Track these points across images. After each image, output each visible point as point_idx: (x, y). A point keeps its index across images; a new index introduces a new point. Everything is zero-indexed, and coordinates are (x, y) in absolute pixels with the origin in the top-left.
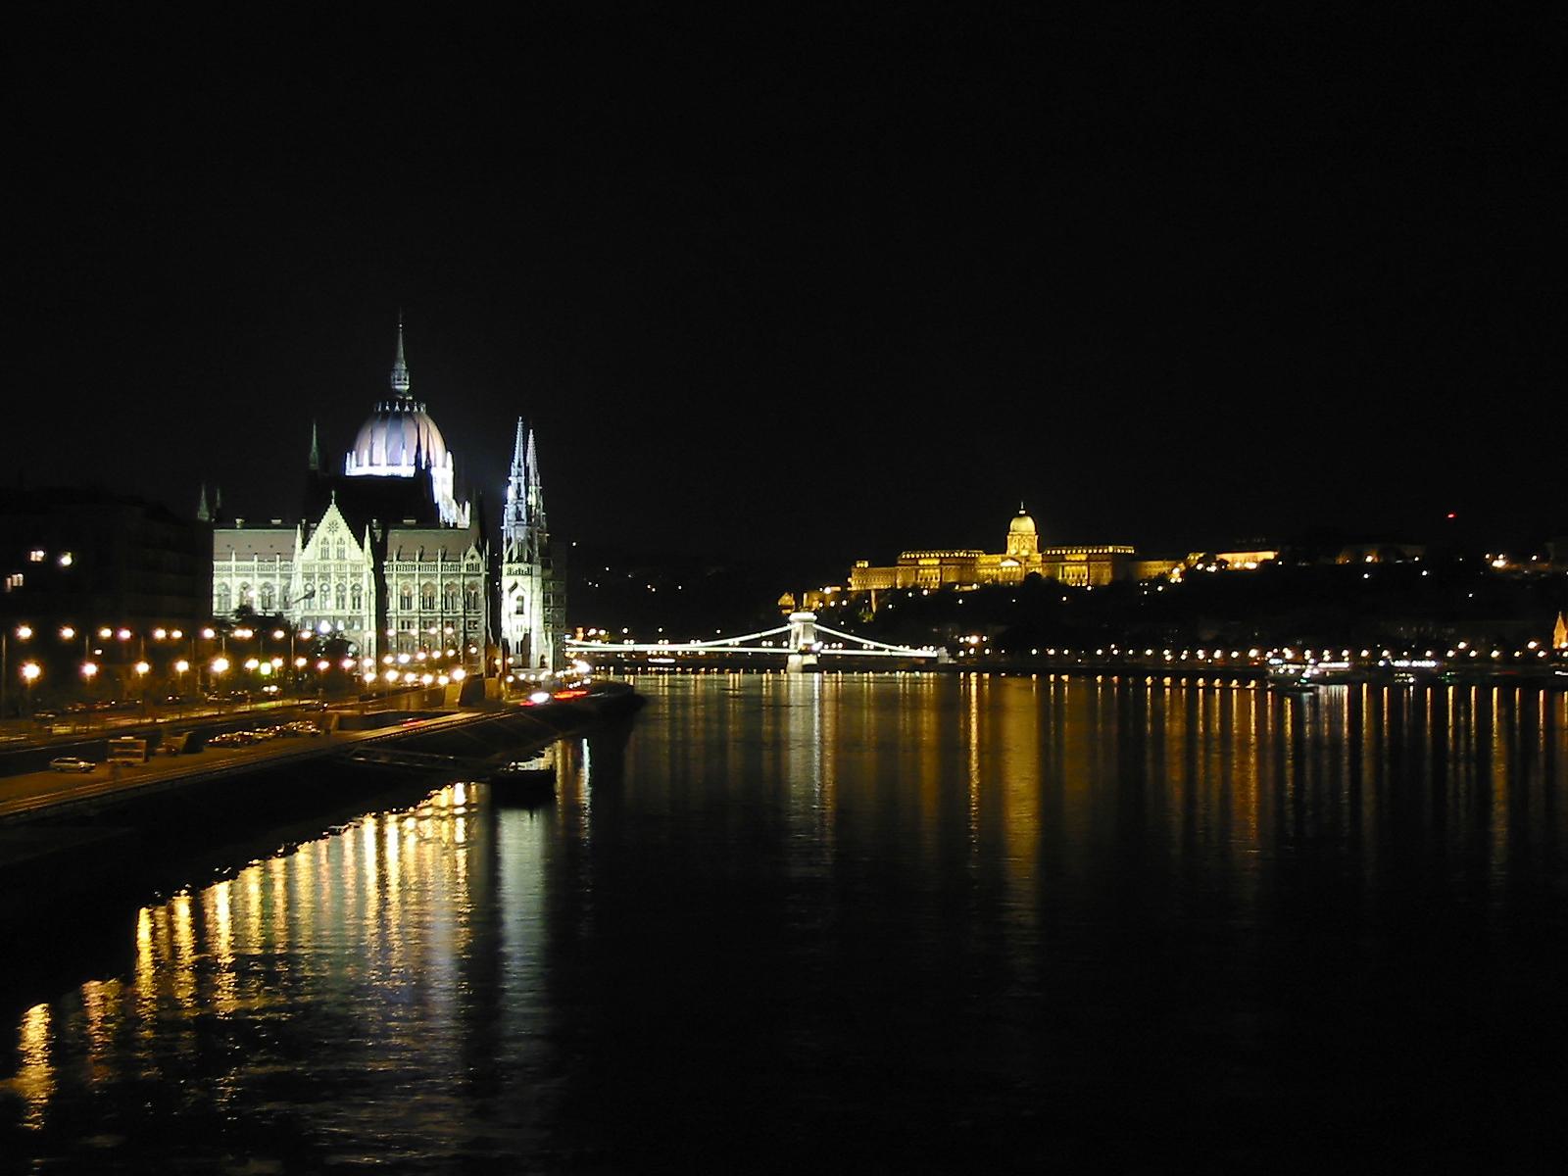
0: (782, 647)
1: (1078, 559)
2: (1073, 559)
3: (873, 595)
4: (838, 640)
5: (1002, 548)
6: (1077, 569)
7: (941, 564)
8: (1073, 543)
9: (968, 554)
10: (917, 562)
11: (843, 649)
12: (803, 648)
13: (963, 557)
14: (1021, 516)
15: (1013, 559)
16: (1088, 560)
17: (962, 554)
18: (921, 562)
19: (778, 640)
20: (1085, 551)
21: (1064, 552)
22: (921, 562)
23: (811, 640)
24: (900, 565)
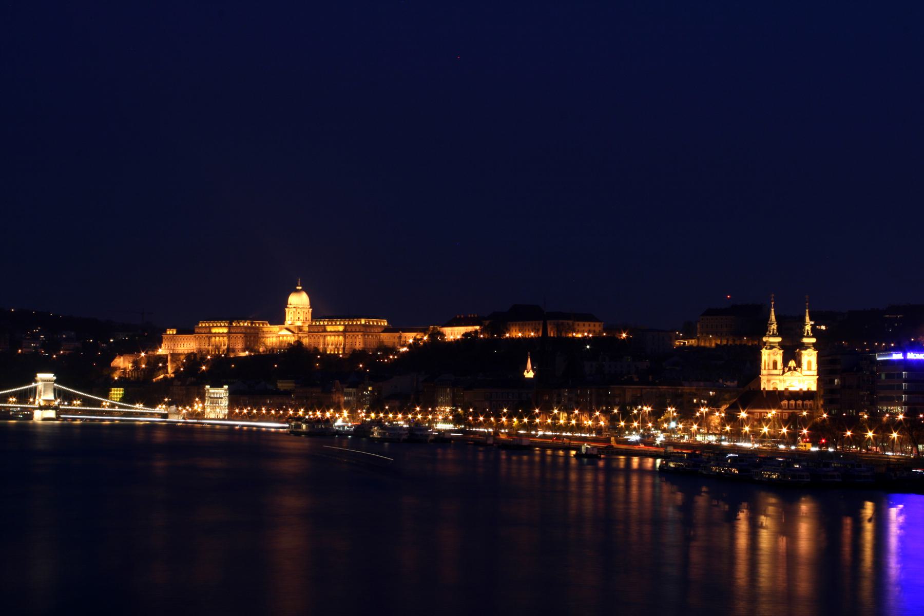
0: (31, 403)
3: (169, 358)
4: (76, 397)
6: (334, 339)
7: (229, 332)
8: (332, 317)
9: (252, 324)
11: (83, 405)
12: (42, 404)
14: (297, 291)
15: (287, 329)
16: (345, 331)
18: (214, 330)
19: (23, 397)
22: (214, 330)
23: (51, 396)
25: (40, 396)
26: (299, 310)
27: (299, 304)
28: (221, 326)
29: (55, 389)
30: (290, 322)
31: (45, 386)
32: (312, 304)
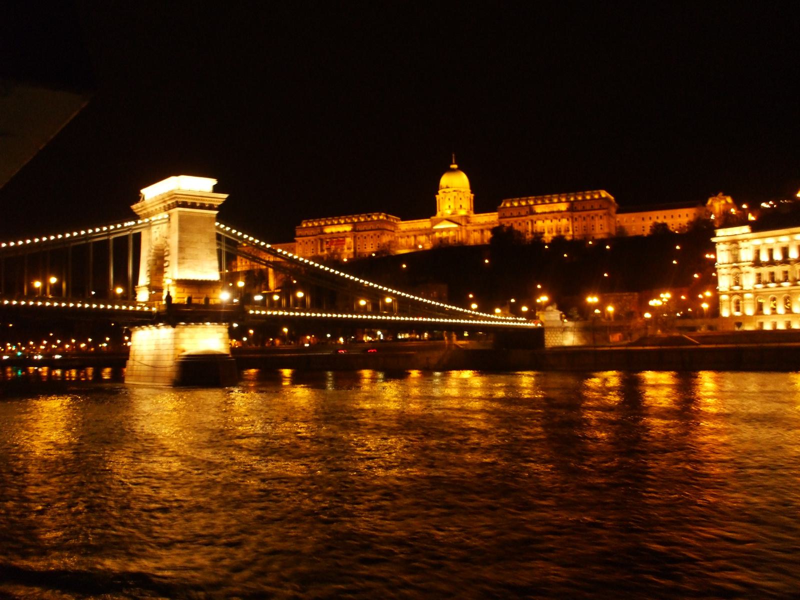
0: (115, 299)
1: (555, 209)
2: (547, 210)
5: (428, 209)
7: (354, 230)
9: (387, 217)
10: (322, 230)
11: (317, 306)
12: (178, 296)
13: (382, 221)
16: (572, 209)
17: (381, 217)
18: (328, 230)
20: (564, 200)
21: (532, 203)
22: (328, 230)
23: (207, 269)
24: (300, 236)
25: (159, 268)
26: (461, 195)
27: (455, 187)
28: (339, 224)
29: (219, 237)
30: (449, 212)
31: (184, 225)
32: (473, 188)
